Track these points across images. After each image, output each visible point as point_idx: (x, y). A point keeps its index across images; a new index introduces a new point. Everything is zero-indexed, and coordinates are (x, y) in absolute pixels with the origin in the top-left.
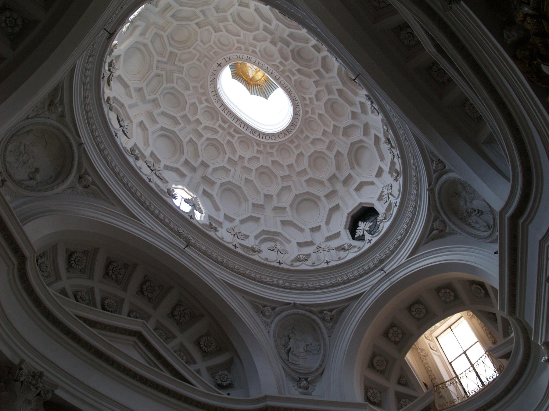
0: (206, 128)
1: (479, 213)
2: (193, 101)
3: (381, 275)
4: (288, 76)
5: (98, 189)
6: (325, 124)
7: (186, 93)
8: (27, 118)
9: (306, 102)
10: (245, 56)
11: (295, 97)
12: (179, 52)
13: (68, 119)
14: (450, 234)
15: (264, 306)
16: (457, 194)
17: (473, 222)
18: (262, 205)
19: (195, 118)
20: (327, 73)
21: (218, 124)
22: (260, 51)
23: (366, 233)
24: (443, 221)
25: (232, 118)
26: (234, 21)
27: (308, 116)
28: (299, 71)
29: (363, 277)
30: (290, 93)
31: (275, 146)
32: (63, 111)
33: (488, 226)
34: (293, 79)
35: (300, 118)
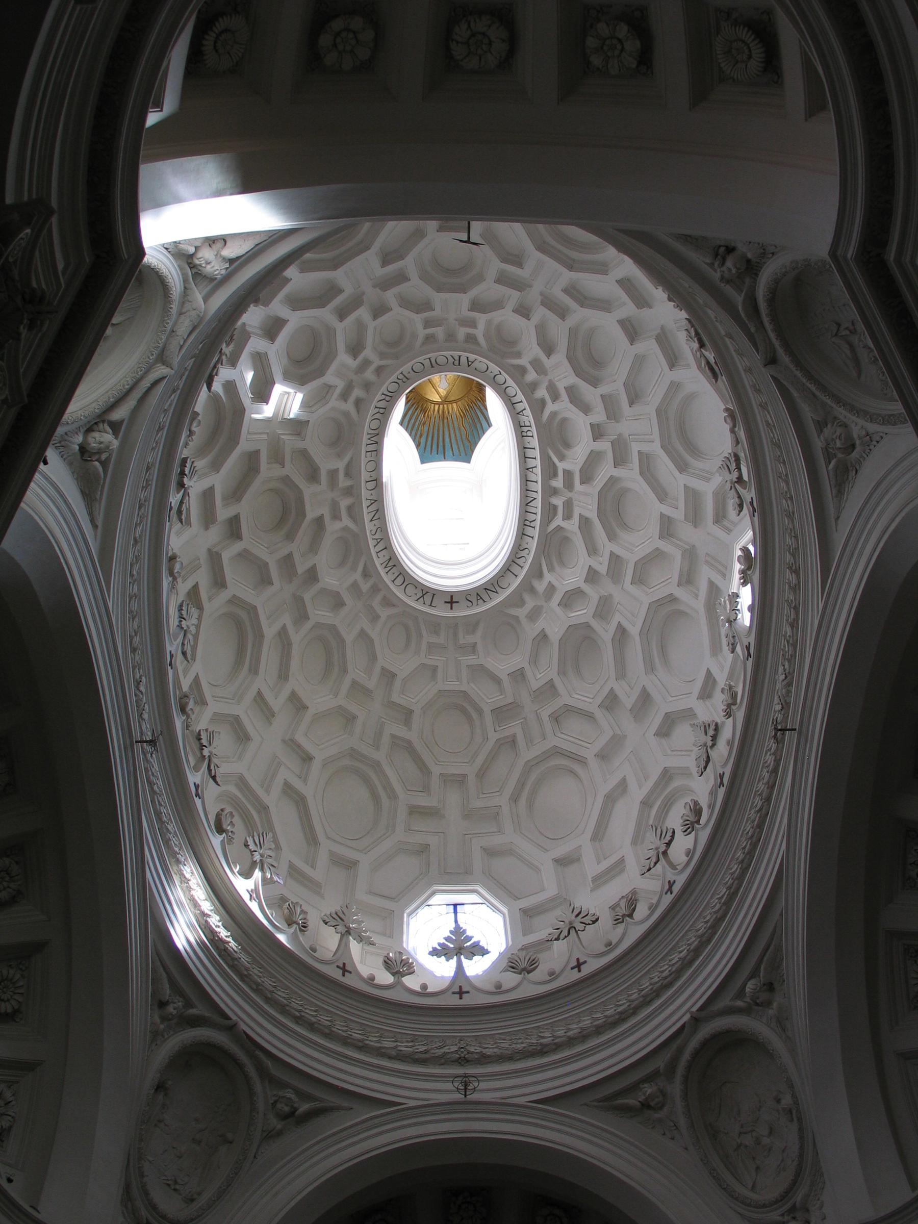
0: (592, 550)
2: (558, 610)
4: (347, 474)
5: (765, 959)
10: (387, 579)
11: (375, 417)
12: (487, 710)
13: (660, 1063)
19: (586, 588)
21: (564, 524)
22: (354, 568)
25: (534, 495)
26: (345, 671)
27: (383, 363)
31: (513, 365)
32: (648, 1079)
34: (341, 465)
35: (406, 369)
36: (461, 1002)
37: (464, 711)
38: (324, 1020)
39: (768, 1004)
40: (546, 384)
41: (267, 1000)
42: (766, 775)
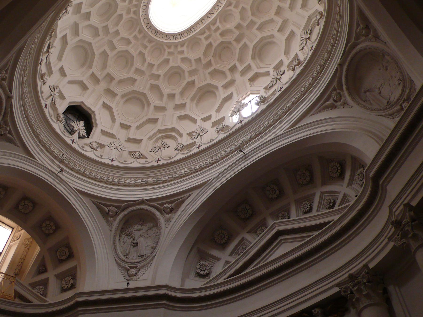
1: (134, 244)
3: (56, 170)
4: (205, 32)
6: (160, 65)
9: (179, 46)
11: (183, 36)
14: (107, 221)
15: (6, 71)
16: (143, 222)
17: (123, 239)
18: (80, 12)
20: (209, 73)
22: (231, 10)
23: (77, 133)
24: (117, 214)
27: (166, 48)
28: (210, 45)
29: (43, 147)
30: (188, 32)
33: (127, 255)
34: (202, 37)
40: (131, 4)
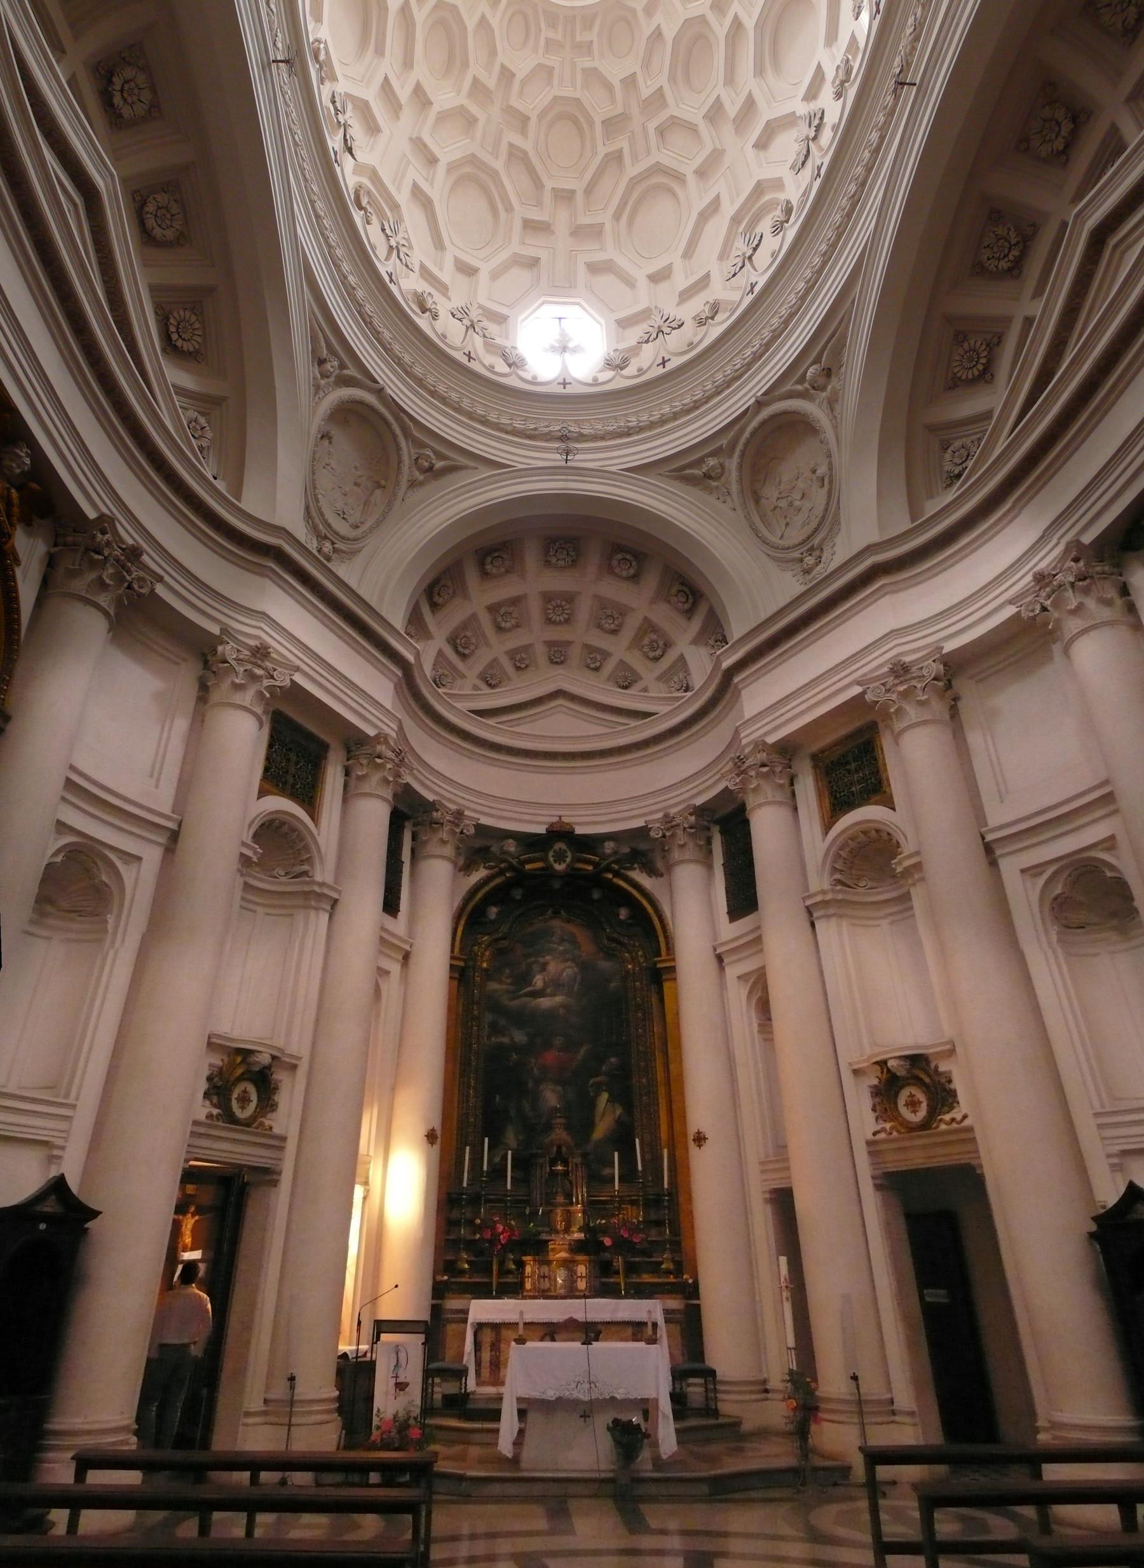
7: (669, 33)
8: (734, 510)
13: (724, 442)
32: (713, 454)
36: (565, 391)
37: (576, 122)
38: (454, 396)
39: (823, 388)
41: (406, 372)
42: (867, 155)
